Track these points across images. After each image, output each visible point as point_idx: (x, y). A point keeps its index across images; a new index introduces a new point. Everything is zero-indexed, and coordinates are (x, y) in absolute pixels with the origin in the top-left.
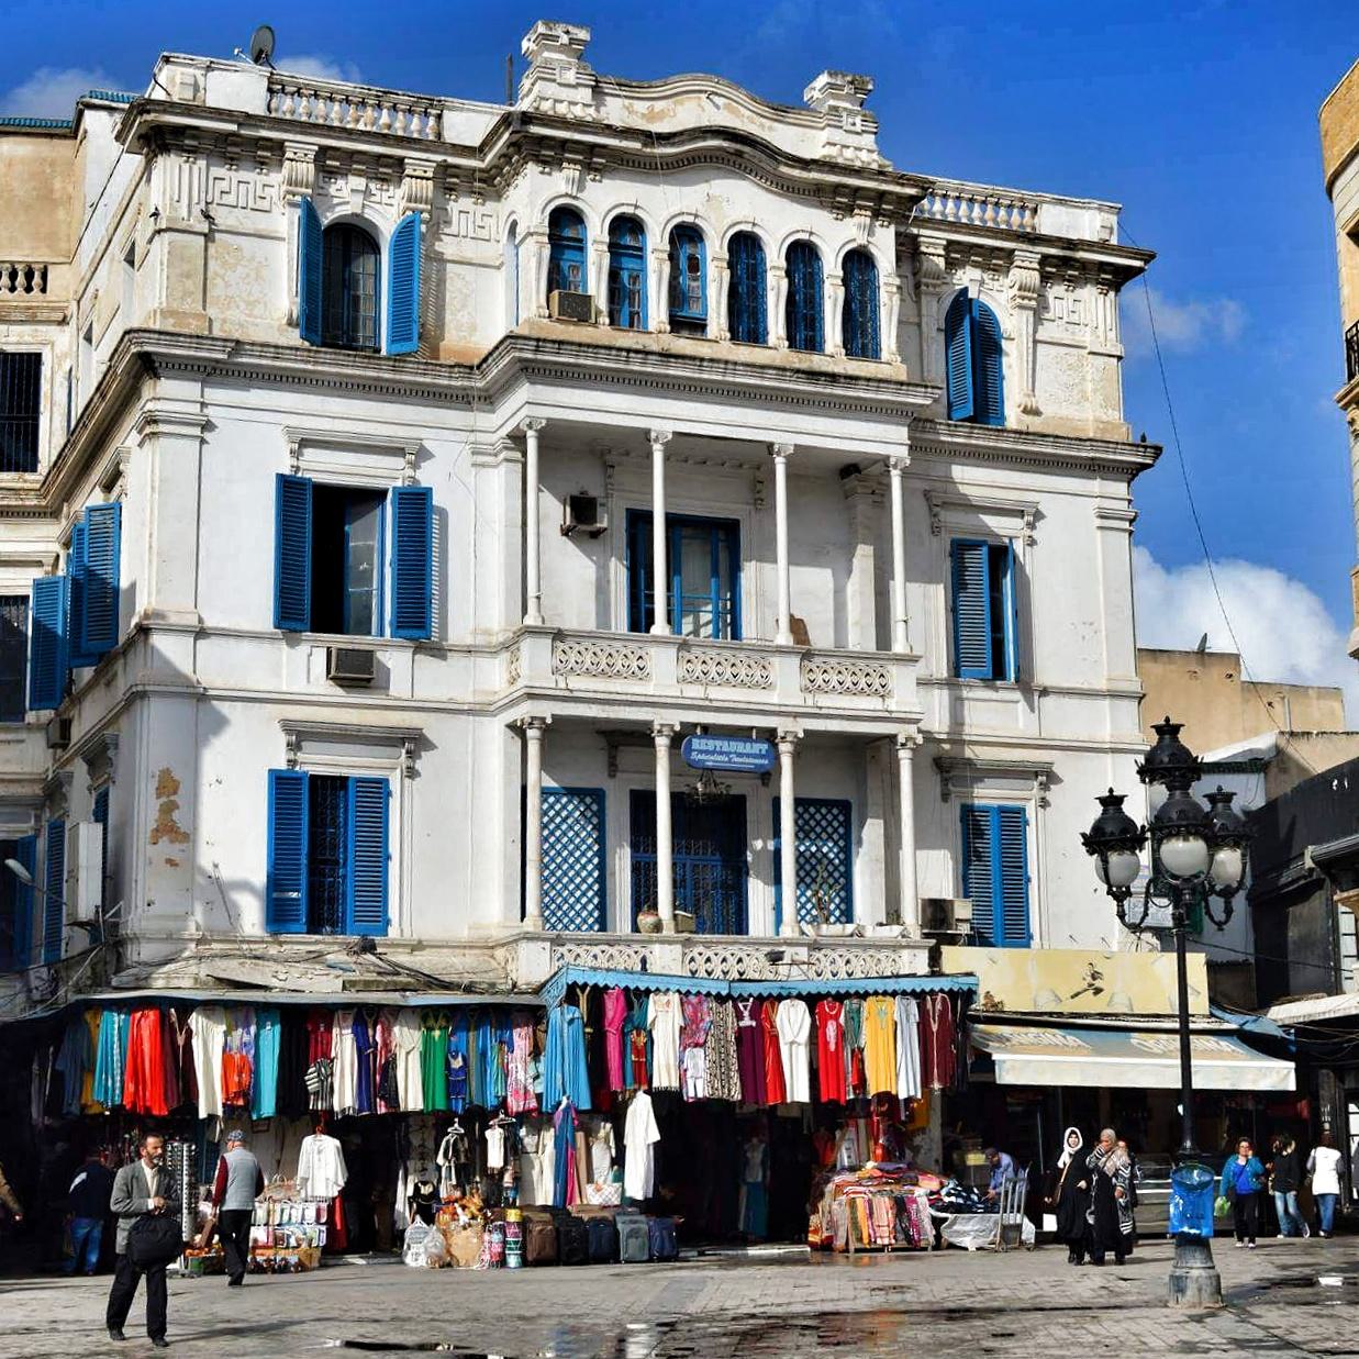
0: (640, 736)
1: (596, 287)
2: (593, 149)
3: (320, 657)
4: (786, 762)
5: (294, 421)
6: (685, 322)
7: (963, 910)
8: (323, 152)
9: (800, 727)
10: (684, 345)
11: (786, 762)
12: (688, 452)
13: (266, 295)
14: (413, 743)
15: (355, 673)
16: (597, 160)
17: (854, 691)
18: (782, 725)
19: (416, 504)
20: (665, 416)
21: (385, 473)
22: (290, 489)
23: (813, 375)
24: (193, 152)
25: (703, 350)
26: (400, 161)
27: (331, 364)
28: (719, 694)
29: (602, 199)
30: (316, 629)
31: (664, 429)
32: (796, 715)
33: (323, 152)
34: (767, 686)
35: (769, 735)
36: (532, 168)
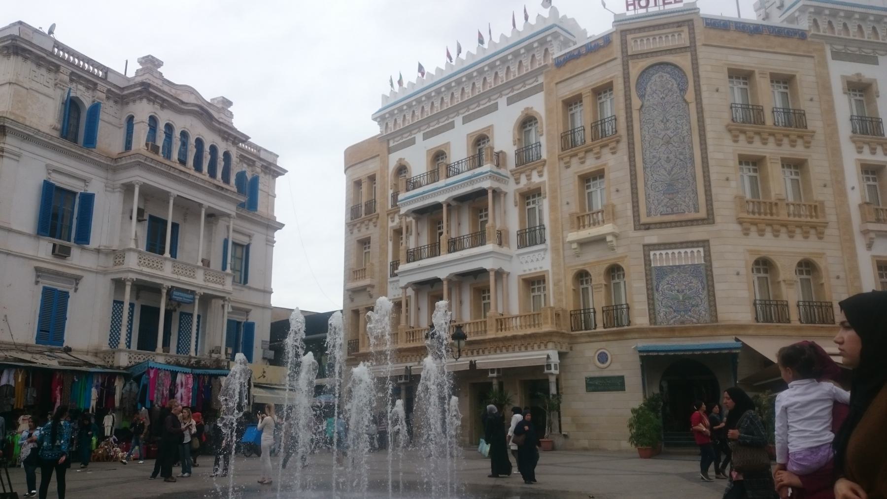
0: (153, 289)
1: (160, 143)
2: (164, 100)
3: (51, 247)
4: (197, 301)
5: (49, 162)
6: (183, 162)
8: (72, 73)
9: (202, 291)
10: (182, 168)
11: (197, 301)
13: (46, 115)
14: (77, 279)
15: (61, 253)
17: (215, 282)
18: (198, 291)
19: (88, 200)
20: (175, 189)
21: (77, 187)
24: (26, 58)
25: (187, 171)
27: (66, 145)
28: (183, 278)
29: (164, 117)
30: (51, 236)
31: (175, 193)
32: (201, 288)
33: (72, 73)
34: (194, 277)
35: (193, 292)
36: (145, 101)
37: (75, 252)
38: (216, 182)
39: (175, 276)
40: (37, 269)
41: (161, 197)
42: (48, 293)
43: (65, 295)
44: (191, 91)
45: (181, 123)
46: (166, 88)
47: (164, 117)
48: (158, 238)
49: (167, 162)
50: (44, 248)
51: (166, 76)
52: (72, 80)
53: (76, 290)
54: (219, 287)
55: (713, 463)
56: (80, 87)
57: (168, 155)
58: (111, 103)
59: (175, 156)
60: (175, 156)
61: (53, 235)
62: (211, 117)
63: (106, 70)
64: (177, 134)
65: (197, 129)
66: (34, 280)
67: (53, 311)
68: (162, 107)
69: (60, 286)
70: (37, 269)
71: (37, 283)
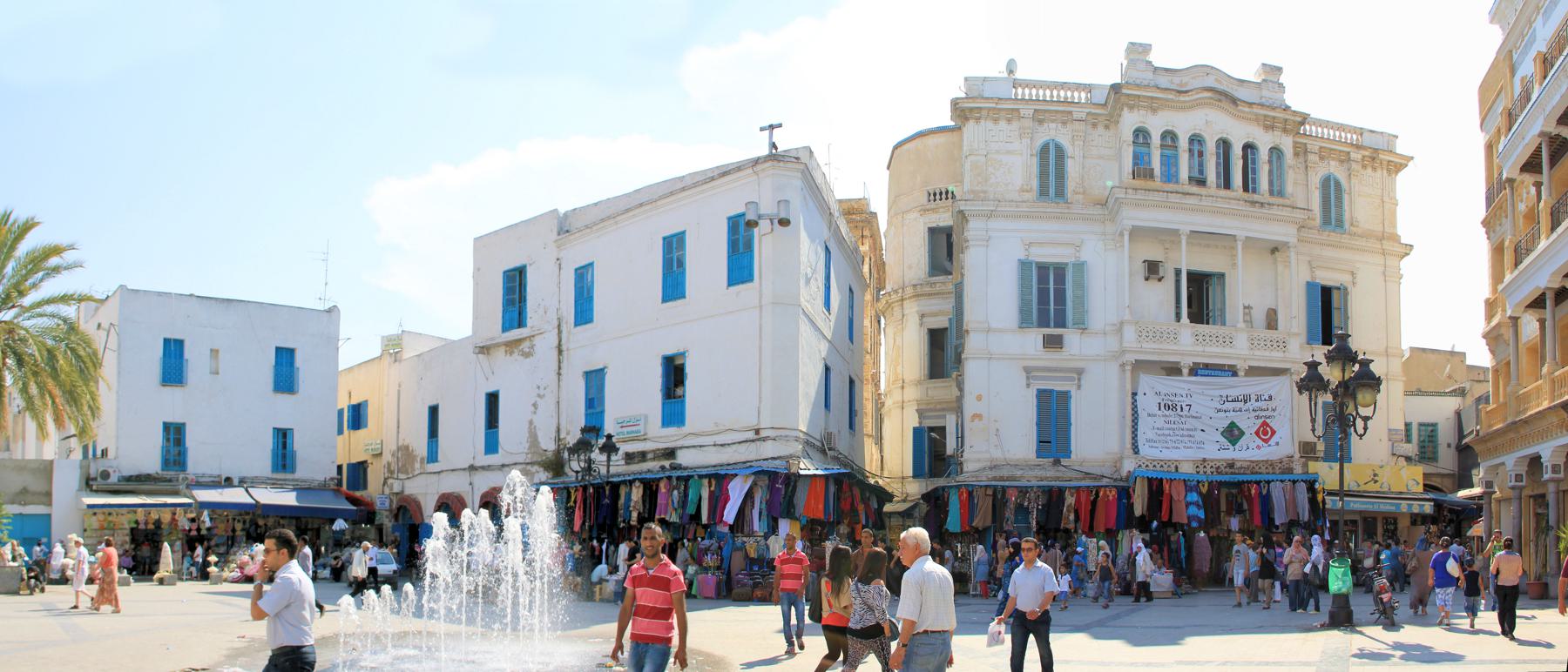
1: (1156, 164)
7: (1321, 447)
10: (1195, 189)
12: (1200, 237)
15: (1053, 343)
16: (1154, 106)
19: (1080, 267)
20: (1184, 221)
22: (1024, 265)
23: (1253, 203)
26: (1070, 113)
31: (1185, 229)
37: (1071, 336)
38: (1256, 197)
39: (1200, 348)
40: (1027, 370)
41: (1168, 236)
42: (1044, 396)
43: (1065, 397)
44: (1208, 70)
45: (1185, 124)
46: (1164, 81)
47: (1157, 125)
48: (1200, 298)
49: (1171, 187)
50: (1035, 337)
51: (1157, 64)
52: (1041, 122)
53: (1079, 387)
54: (1280, 354)
55: (1032, 637)
56: (1053, 125)
57: (1170, 175)
58: (1101, 129)
59: (1184, 174)
60: (1184, 174)
61: (1043, 322)
62: (1234, 101)
63: (1089, 88)
64: (1183, 143)
65: (1216, 124)
66: (1024, 382)
67: (1053, 416)
68: (1154, 111)
69: (1058, 386)
70: (1027, 370)
71: (1028, 385)
